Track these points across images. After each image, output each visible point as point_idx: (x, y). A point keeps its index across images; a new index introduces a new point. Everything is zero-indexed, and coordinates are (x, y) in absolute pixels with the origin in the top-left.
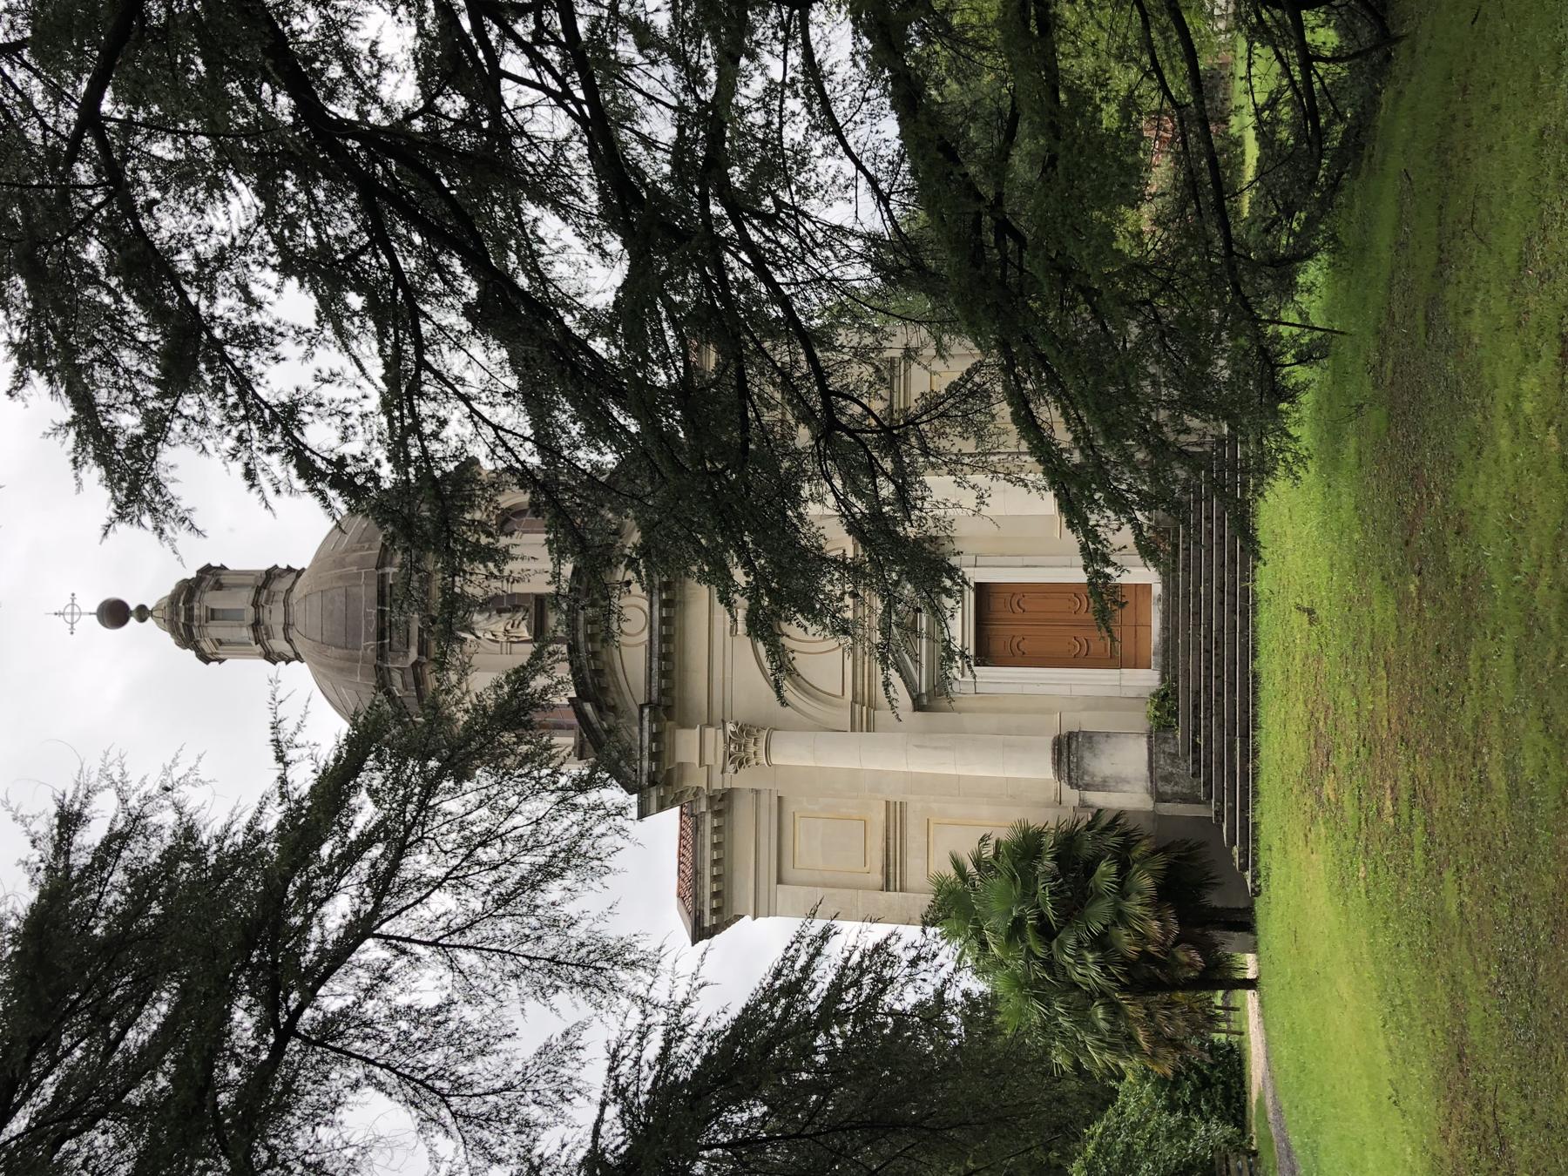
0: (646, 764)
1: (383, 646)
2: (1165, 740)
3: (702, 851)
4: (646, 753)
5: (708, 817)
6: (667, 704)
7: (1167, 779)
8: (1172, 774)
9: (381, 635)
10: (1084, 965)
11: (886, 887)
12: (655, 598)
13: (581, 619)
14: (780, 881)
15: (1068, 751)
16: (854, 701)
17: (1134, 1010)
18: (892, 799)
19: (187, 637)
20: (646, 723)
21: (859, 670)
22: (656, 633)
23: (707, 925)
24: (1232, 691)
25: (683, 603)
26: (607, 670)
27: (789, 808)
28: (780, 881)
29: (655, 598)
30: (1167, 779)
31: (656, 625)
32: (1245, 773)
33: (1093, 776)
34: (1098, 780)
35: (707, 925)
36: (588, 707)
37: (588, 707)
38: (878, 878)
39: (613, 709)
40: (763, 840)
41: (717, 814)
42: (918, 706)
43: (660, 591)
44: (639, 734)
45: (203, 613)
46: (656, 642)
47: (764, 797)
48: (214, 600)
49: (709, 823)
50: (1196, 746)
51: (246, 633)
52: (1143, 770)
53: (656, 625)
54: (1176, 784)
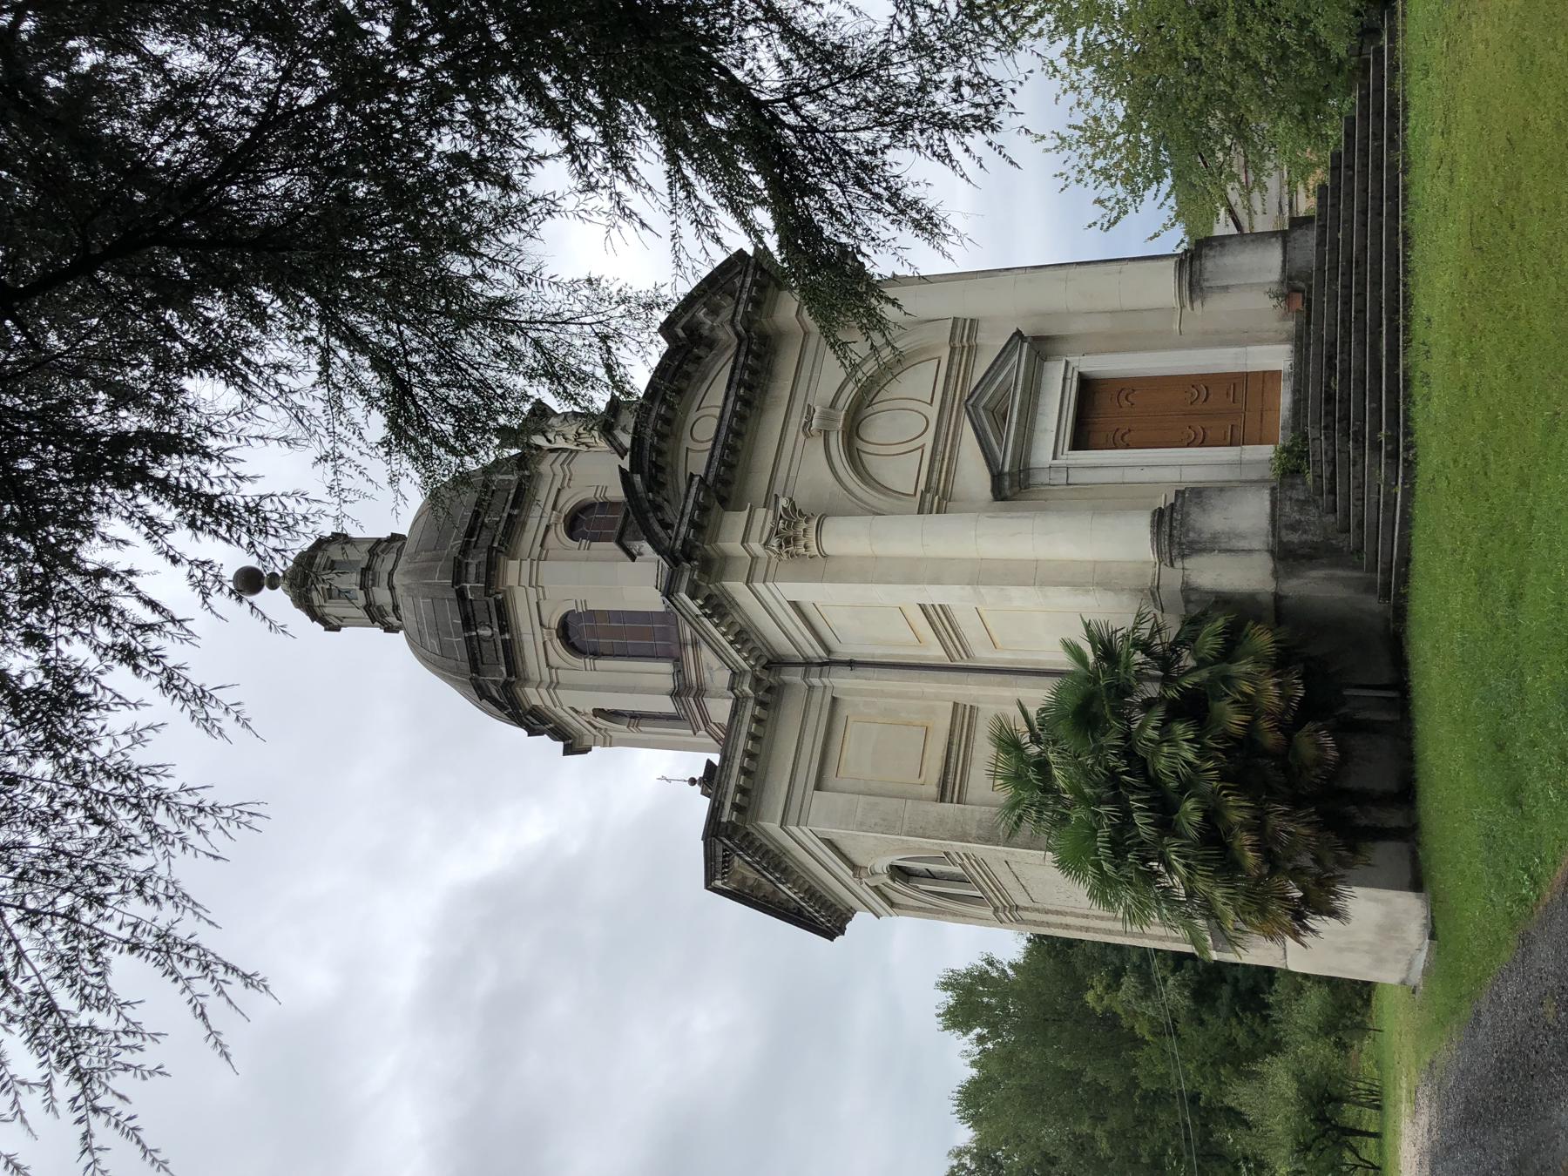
0: (683, 529)
1: (468, 543)
2: (1292, 487)
3: (737, 737)
4: (686, 520)
5: (751, 703)
6: (724, 486)
7: (1293, 527)
8: (1300, 522)
9: (470, 533)
10: (1172, 742)
11: (942, 798)
12: (732, 392)
13: (654, 414)
14: (818, 787)
15: (1173, 526)
16: (928, 489)
17: (1237, 811)
18: (961, 701)
19: (303, 602)
20: (693, 491)
21: (937, 465)
22: (726, 423)
23: (724, 819)
24: (1377, 284)
25: (761, 411)
26: (668, 470)
27: (844, 711)
28: (818, 787)
29: (732, 392)
30: (1293, 527)
31: (727, 416)
32: (1393, 378)
33: (1200, 532)
34: (1206, 536)
35: (724, 819)
36: (637, 478)
37: (637, 478)
38: (933, 790)
39: (662, 485)
40: (808, 740)
41: (762, 704)
42: (999, 493)
43: (739, 388)
44: (683, 504)
45: (324, 561)
46: (724, 432)
47: (817, 696)
48: (335, 553)
49: (750, 709)
50: (1330, 398)
51: (362, 613)
52: (1264, 523)
53: (727, 416)
54: (1305, 532)
